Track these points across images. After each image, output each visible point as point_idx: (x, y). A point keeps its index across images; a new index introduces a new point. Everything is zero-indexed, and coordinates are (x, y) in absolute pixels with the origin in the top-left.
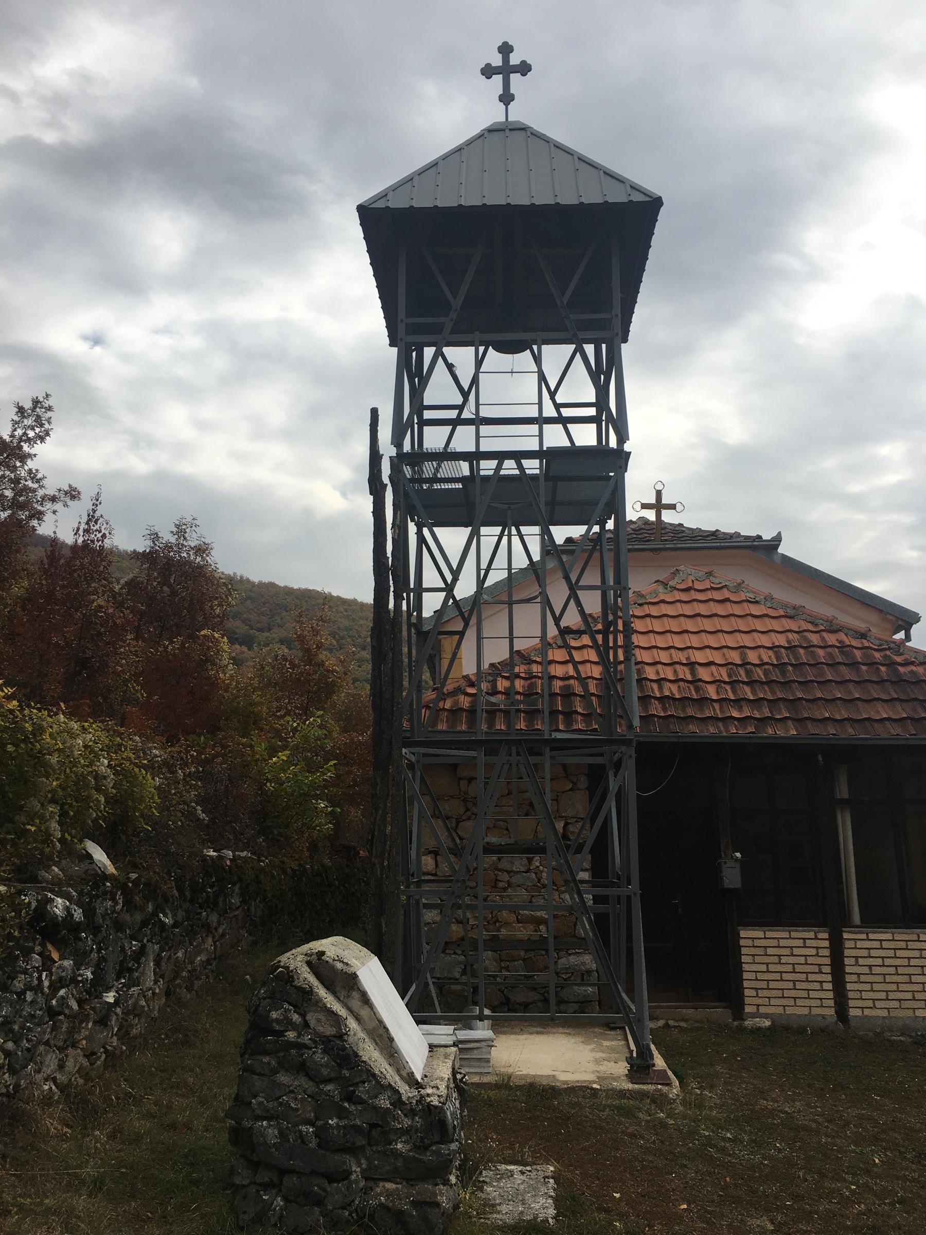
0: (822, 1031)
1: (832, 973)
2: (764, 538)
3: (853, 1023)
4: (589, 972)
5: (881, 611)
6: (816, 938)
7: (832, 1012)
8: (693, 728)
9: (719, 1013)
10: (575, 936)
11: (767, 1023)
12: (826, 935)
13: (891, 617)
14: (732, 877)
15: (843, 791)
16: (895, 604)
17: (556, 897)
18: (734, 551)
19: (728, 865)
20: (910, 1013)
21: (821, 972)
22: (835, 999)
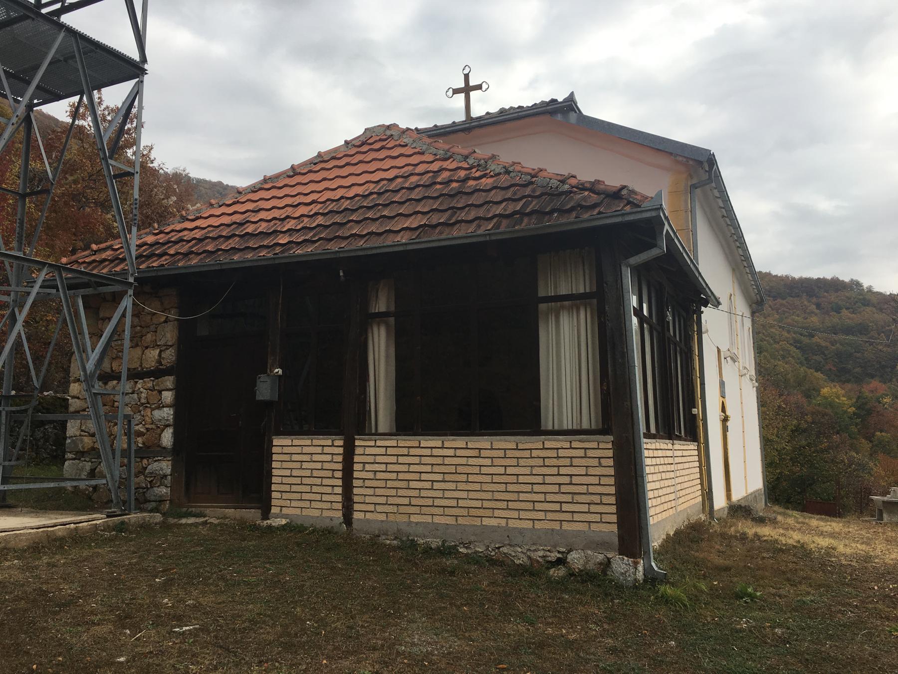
0: (328, 532)
1: (343, 478)
2: (560, 100)
3: (355, 526)
4: (165, 476)
5: (671, 154)
6: (333, 445)
7: (339, 514)
8: (249, 256)
9: (251, 514)
10: (159, 446)
11: (284, 522)
12: (341, 443)
13: (681, 159)
14: (265, 390)
15: (381, 304)
16: (686, 144)
17: (149, 414)
18: (527, 120)
19: (262, 380)
20: (405, 518)
21: (333, 477)
22: (343, 503)
